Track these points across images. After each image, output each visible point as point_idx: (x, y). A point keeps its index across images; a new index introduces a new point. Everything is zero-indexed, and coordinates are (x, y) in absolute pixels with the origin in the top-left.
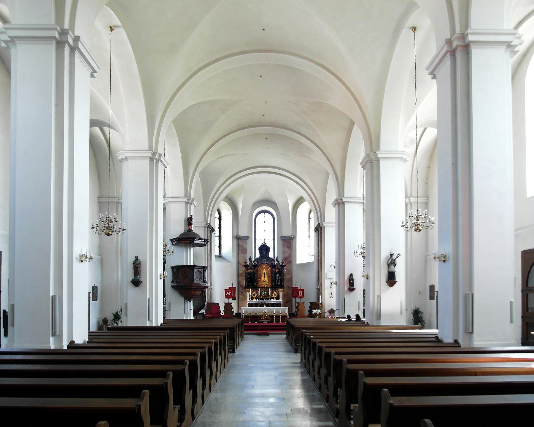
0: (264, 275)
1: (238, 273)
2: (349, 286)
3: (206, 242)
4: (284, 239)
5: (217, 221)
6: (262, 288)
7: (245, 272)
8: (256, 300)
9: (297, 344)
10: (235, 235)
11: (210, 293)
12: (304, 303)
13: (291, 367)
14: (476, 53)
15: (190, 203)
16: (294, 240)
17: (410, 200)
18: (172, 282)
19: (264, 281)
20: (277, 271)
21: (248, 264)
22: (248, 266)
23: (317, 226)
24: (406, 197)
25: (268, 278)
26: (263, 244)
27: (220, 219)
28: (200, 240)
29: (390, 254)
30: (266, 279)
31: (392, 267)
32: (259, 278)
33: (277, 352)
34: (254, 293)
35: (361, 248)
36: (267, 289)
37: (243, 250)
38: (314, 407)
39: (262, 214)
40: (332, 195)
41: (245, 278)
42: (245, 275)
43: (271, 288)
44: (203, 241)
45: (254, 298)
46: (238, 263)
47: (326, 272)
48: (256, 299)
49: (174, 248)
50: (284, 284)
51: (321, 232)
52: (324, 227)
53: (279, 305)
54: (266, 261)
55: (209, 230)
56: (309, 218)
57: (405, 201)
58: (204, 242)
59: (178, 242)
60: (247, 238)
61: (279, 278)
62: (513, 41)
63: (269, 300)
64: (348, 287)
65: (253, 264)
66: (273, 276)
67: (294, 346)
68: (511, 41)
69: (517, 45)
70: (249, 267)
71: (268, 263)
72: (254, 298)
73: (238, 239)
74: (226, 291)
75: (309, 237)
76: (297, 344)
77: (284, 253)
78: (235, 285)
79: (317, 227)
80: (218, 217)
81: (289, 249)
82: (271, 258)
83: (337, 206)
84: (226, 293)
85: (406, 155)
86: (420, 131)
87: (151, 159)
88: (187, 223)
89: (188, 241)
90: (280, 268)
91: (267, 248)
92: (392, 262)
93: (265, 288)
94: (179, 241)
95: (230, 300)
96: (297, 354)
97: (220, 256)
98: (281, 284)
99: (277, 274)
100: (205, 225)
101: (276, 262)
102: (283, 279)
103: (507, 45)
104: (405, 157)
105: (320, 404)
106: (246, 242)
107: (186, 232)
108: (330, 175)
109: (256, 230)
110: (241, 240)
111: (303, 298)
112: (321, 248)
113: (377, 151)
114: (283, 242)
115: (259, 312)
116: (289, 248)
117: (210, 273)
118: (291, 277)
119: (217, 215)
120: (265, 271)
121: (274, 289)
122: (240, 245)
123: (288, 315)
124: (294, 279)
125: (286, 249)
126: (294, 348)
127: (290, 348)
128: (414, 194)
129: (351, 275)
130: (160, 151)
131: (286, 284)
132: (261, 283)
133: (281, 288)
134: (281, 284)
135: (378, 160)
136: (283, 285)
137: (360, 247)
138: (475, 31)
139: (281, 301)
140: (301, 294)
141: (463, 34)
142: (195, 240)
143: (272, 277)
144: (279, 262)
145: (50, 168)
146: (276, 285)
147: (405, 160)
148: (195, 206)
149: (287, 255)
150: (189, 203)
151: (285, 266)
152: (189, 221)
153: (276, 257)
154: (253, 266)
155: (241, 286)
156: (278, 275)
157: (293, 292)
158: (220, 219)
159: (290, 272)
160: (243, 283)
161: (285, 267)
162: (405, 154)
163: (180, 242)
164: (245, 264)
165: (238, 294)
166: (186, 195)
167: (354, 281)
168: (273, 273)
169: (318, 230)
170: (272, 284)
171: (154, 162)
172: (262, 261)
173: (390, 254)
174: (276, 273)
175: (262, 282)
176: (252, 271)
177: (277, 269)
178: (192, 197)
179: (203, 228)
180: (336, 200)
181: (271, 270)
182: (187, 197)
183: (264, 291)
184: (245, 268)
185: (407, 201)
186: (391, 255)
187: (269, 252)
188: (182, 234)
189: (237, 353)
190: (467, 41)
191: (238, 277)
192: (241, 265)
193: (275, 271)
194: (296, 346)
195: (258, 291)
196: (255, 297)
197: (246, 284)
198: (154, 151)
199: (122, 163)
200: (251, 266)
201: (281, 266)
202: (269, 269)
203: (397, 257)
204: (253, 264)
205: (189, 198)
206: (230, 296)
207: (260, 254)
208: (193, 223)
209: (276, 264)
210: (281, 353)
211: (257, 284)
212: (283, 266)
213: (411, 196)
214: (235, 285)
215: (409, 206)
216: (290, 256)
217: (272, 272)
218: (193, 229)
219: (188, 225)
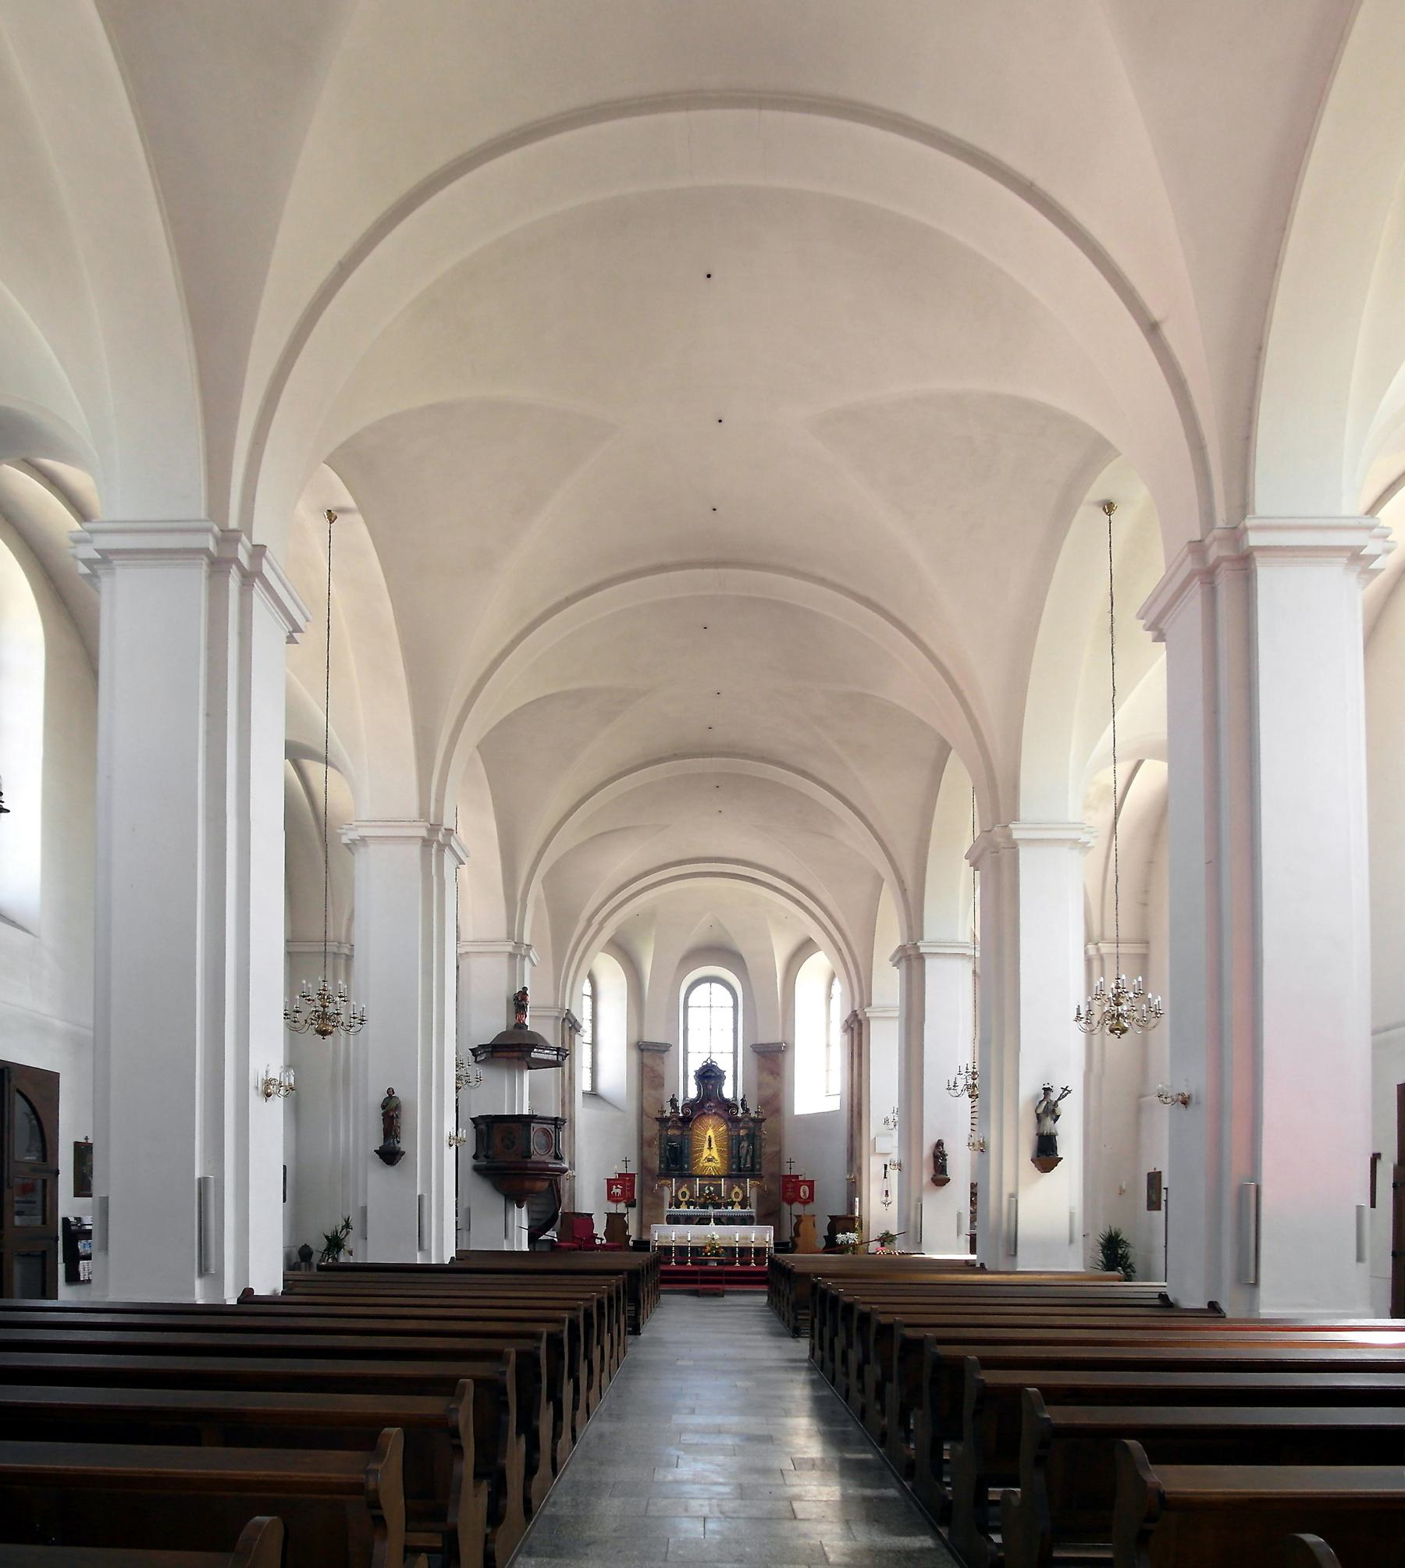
0: (710, 1145)
1: (642, 1139)
2: (932, 1171)
3: (561, 1055)
4: (761, 1050)
5: (587, 1003)
6: (701, 1177)
8: (688, 1208)
9: (799, 1317)
10: (635, 1039)
11: (570, 1187)
12: (814, 1216)
13: (786, 1369)
14: (1266, 575)
15: (521, 955)
16: (788, 1056)
17: (1098, 950)
18: (475, 1157)
19: (709, 1160)
20: (742, 1132)
21: (668, 1114)
22: (667, 1119)
23: (850, 1016)
24: (1089, 939)
25: (720, 1151)
27: (594, 997)
28: (548, 1051)
29: (1044, 1089)
30: (715, 1153)
31: (1049, 1121)
32: (696, 1152)
33: (748, 1334)
34: (684, 1189)
35: (967, 1074)
37: (653, 1077)
38: (848, 1456)
39: (705, 987)
40: (890, 936)
41: (660, 1153)
42: (660, 1144)
43: (728, 1177)
44: (556, 1053)
45: (684, 1203)
46: (642, 1112)
47: (872, 1137)
48: (689, 1204)
49: (480, 1070)
51: (860, 1034)
52: (868, 1020)
54: (716, 1107)
55: (567, 1025)
56: (829, 997)
57: (1086, 952)
58: (557, 1055)
59: (489, 1054)
61: (748, 1151)
62: (1366, 547)
63: (723, 1210)
64: (931, 1176)
65: (681, 1115)
66: (732, 1147)
67: (791, 1319)
68: (1360, 546)
69: (1378, 556)
70: (670, 1123)
71: (720, 1112)
72: (684, 1203)
73: (642, 1050)
74: (610, 1183)
75: (828, 1046)
76: (799, 1317)
77: (760, 1086)
78: (633, 1169)
79: (850, 1022)
80: (590, 994)
81: (775, 1078)
82: (727, 1101)
83: (903, 964)
84: (610, 1189)
85: (1087, 833)
86: (1124, 768)
87: (426, 843)
88: (513, 1008)
89: (516, 1054)
90: (751, 1124)
91: (718, 1074)
92: (1047, 1109)
93: (713, 1176)
94: (492, 1052)
95: (621, 1208)
96: (801, 1340)
97: (593, 1094)
98: (753, 1169)
99: (743, 1140)
100: (557, 1014)
102: (760, 1153)
103: (1349, 554)
104: (1084, 838)
105: (864, 1451)
106: (662, 1059)
107: (511, 1028)
108: (885, 885)
109: (689, 1028)
110: (649, 1053)
112: (860, 1075)
113: (1011, 823)
114: (759, 1060)
115: (698, 1238)
117: (570, 1136)
118: (778, 1149)
119: (587, 988)
120: (710, 1133)
121: (736, 1180)
122: (646, 1065)
123: (772, 1246)
124: (788, 1155)
125: (768, 1078)
126: (791, 1326)
127: (780, 1326)
128: (1110, 933)
129: (940, 1144)
130: (448, 823)
131: (766, 1168)
133: (752, 1177)
134: (753, 1169)
135: (1014, 847)
136: (760, 1170)
137: (963, 1070)
138: (1266, 522)
139: (751, 1212)
141: (1235, 528)
142: (535, 1050)
143: (730, 1149)
144: (748, 1110)
145: (195, 866)
146: (740, 1170)
147: (1084, 847)
148: (534, 965)
149: (769, 1092)
150: (519, 956)
151: (763, 1120)
152: (519, 1002)
153: (740, 1096)
154: (681, 1119)
155: (650, 1171)
156: (745, 1144)
157: (785, 1188)
158: (594, 997)
159: (777, 1138)
160: (655, 1164)
161: (763, 1123)
162: (1087, 829)
163: (496, 1055)
164: (659, 1116)
166: (510, 936)
167: (946, 1160)
168: (732, 1140)
169: (852, 1029)
170: (730, 1168)
171: (434, 851)
172: (703, 1107)
173: (1044, 1089)
174: (740, 1139)
175: (703, 1162)
176: (677, 1132)
177: (743, 1128)
178: (527, 941)
179: (551, 1022)
180: (902, 948)
181: (728, 1130)
182: (513, 940)
183: (710, 1185)
184: (660, 1125)
185: (1092, 951)
186: (1047, 1091)
187: (721, 1085)
188: (501, 1035)
189: (643, 1336)
190: (1245, 547)
191: (642, 1148)
192: (649, 1117)
194: (796, 1319)
196: (686, 1199)
198: (432, 822)
199: (354, 854)
200: (674, 1119)
201: (753, 1120)
202: (721, 1129)
203: (1062, 1097)
204: (681, 1115)
205: (519, 944)
207: (699, 1089)
208: (528, 1006)
209: (739, 1115)
210: (759, 1337)
212: (758, 1122)
213: (1102, 938)
214: (633, 1169)
215: (1096, 965)
216: (778, 1095)
217: (730, 1138)
218: (527, 1022)
219: (517, 1012)
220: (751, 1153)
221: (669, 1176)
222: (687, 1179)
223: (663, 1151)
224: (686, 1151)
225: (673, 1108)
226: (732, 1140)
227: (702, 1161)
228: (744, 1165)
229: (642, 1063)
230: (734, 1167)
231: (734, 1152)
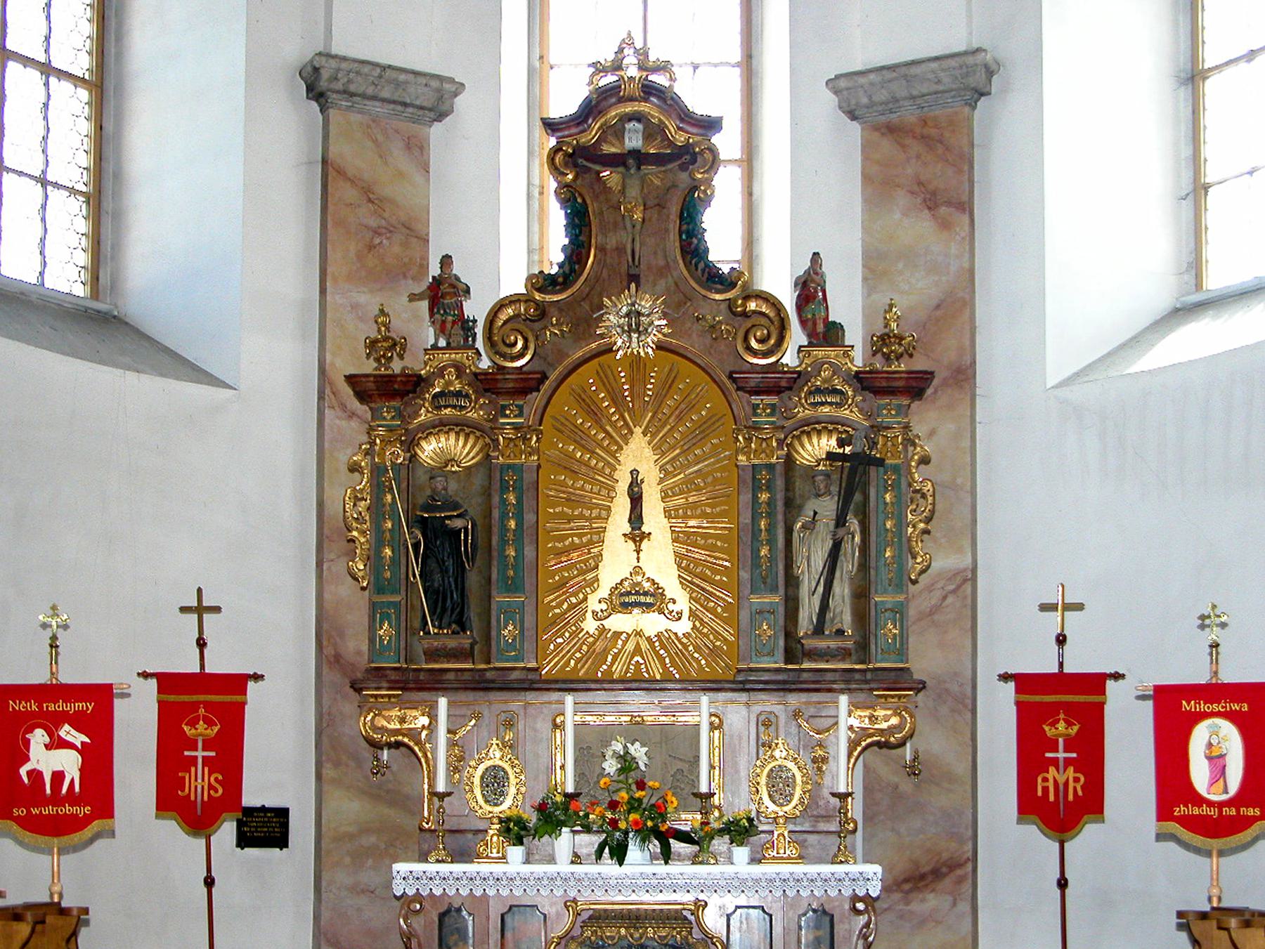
0: (636, 517)
7: (378, 471)
22: (413, 385)
26: (610, 79)
37: (376, 232)
50: (904, 637)
60: (426, 98)
81: (945, 225)
93: (658, 681)
101: (797, 336)
106: (417, 149)
114: (866, 148)
116: (943, 210)
122: (341, 172)
132: (590, 625)
140: (1217, 763)
193: (789, 461)
197: (385, 630)
206: (71, 798)
211: (534, 636)
225: (442, 330)
226: (756, 488)
227: (593, 604)
229: (325, 162)
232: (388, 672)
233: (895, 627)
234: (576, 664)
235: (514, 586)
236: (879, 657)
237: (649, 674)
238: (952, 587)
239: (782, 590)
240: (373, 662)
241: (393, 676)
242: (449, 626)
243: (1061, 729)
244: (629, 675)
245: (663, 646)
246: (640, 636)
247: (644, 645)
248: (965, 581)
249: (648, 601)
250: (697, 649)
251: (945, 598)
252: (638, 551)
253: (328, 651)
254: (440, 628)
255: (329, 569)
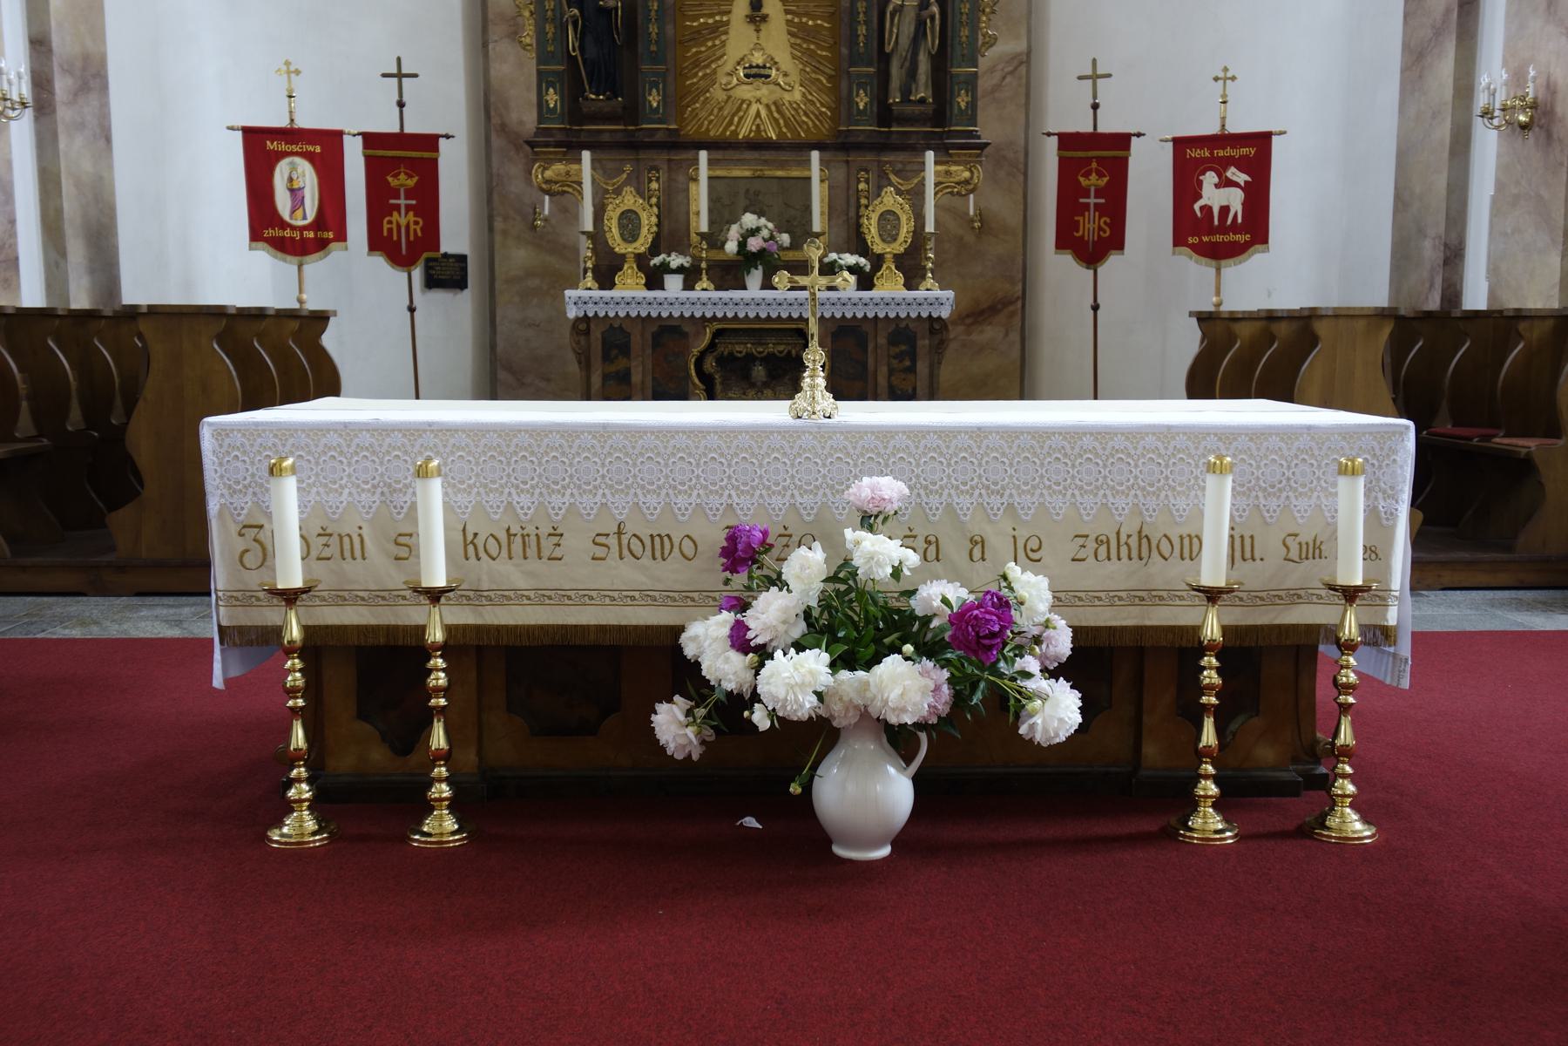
6: (721, 147)
19: (757, 74)
25: (798, 33)
30: (776, 44)
32: (698, 36)
36: (784, 156)
41: (540, 33)
43: (839, 146)
50: (973, 105)
53: (923, 343)
61: (920, 25)
98: (940, 112)
111: (1255, 262)
121: (870, 157)
132: (718, 94)
136: (971, 116)
139: (939, 302)
165: (491, 229)
170: (842, 105)
191: (485, 45)
195: (681, 178)
197: (552, 98)
211: (678, 100)
220: (932, 42)
221: (570, 148)
222: (660, 158)
223: (550, 29)
224: (653, 29)
228: (905, 99)
230: (862, 101)
231: (862, 30)
232: (554, 132)
233: (967, 96)
234: (708, 126)
235: (656, 58)
236: (954, 121)
237: (767, 134)
238: (1010, 69)
239: (876, 65)
240: (541, 124)
241: (560, 137)
242: (603, 95)
243: (1093, 181)
244: (752, 134)
245: (779, 111)
246: (760, 103)
247: (763, 113)
248: (1021, 63)
249: (766, 73)
250: (806, 114)
251: (1004, 78)
252: (758, 31)
253: (495, 120)
254: (598, 95)
255: (494, 49)
